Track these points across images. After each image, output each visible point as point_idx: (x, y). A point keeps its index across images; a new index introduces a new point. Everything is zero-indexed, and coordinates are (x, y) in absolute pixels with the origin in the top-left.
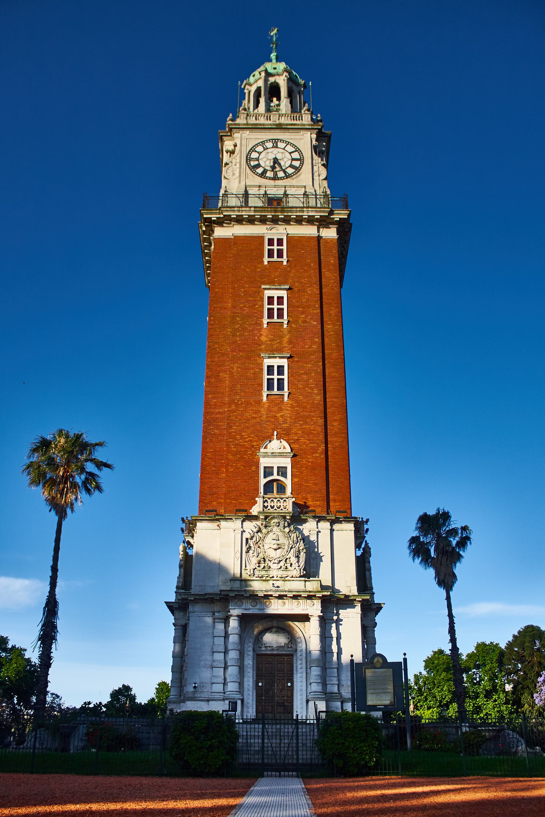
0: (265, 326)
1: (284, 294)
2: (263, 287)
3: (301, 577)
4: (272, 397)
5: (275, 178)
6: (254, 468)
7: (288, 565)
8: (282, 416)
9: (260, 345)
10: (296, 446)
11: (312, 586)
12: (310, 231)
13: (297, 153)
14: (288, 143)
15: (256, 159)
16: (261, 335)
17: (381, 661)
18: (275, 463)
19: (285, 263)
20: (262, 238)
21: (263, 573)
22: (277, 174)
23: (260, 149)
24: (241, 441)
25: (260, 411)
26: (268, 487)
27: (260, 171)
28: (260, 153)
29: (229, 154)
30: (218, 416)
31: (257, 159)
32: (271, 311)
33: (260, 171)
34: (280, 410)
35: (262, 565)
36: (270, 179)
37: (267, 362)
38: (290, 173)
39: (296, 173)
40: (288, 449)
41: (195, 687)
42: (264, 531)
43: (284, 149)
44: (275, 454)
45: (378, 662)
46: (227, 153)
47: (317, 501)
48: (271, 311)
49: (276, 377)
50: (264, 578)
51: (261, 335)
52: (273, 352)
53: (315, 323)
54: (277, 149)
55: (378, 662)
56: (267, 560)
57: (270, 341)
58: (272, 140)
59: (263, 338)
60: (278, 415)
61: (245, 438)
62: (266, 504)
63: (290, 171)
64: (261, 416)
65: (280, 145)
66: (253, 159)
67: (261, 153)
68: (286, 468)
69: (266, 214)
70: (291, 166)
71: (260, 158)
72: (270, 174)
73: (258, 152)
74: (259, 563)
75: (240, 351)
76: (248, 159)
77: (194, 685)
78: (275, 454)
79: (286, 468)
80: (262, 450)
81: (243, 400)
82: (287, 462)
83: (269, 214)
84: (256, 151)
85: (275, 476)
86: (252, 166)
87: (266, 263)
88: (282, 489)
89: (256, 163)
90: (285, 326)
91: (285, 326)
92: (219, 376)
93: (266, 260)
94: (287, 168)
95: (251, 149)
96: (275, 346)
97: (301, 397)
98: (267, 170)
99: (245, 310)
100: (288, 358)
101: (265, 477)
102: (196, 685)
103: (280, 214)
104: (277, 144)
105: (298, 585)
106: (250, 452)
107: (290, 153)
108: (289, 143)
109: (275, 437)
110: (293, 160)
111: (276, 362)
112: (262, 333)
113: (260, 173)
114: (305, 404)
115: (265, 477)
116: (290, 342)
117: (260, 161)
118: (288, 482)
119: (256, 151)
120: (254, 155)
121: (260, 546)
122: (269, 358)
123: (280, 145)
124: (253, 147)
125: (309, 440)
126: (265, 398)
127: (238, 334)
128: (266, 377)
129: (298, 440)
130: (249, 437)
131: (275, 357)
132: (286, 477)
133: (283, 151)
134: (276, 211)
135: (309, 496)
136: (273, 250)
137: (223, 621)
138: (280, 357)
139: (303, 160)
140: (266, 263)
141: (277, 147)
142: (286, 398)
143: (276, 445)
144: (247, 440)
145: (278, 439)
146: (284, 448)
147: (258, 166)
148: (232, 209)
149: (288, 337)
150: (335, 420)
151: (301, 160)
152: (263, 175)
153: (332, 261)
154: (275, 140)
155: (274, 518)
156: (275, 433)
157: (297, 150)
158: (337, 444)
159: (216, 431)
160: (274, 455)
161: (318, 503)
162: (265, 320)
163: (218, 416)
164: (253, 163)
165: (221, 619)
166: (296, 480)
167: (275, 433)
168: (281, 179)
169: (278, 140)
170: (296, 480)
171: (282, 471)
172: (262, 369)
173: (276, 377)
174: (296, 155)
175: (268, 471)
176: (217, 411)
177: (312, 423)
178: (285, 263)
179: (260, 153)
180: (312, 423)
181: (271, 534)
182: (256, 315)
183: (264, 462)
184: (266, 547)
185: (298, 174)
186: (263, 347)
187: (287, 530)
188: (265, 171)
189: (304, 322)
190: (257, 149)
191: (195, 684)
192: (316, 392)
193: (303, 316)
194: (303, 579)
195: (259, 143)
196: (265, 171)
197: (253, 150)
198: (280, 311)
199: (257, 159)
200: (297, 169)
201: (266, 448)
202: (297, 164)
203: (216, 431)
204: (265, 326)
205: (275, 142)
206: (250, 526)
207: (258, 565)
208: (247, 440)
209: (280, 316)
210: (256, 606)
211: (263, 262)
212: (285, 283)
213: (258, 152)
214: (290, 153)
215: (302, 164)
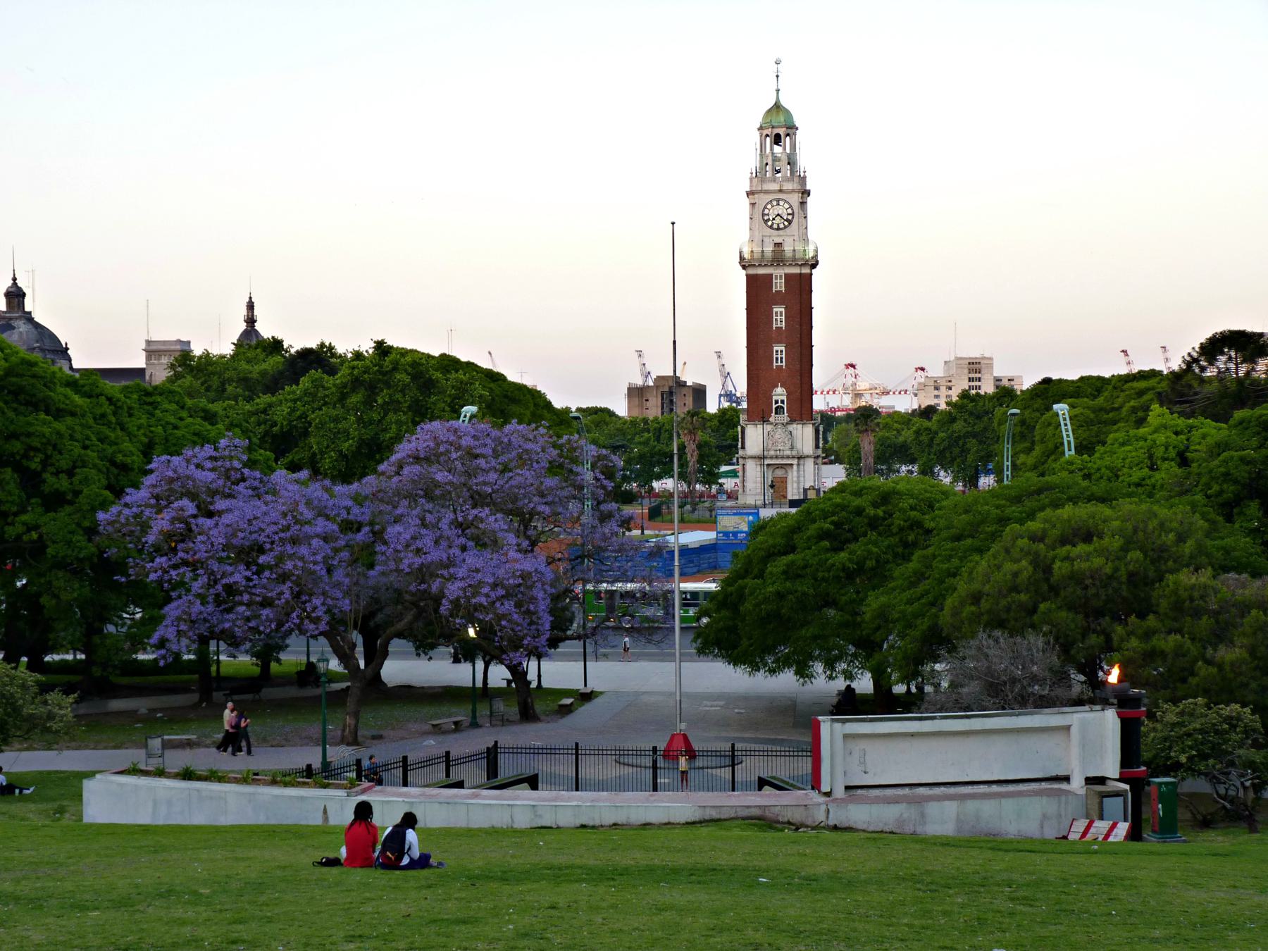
5: (778, 229)
11: (794, 453)
12: (796, 270)
18: (780, 398)
44: (780, 394)
76: (763, 215)
78: (780, 394)
82: (785, 398)
105: (788, 453)
143: (779, 390)
151: (792, 214)
152: (771, 227)
171: (782, 402)
174: (790, 211)
175: (777, 402)
183: (775, 398)
197: (765, 208)
200: (790, 222)
205: (778, 200)
206: (768, 428)
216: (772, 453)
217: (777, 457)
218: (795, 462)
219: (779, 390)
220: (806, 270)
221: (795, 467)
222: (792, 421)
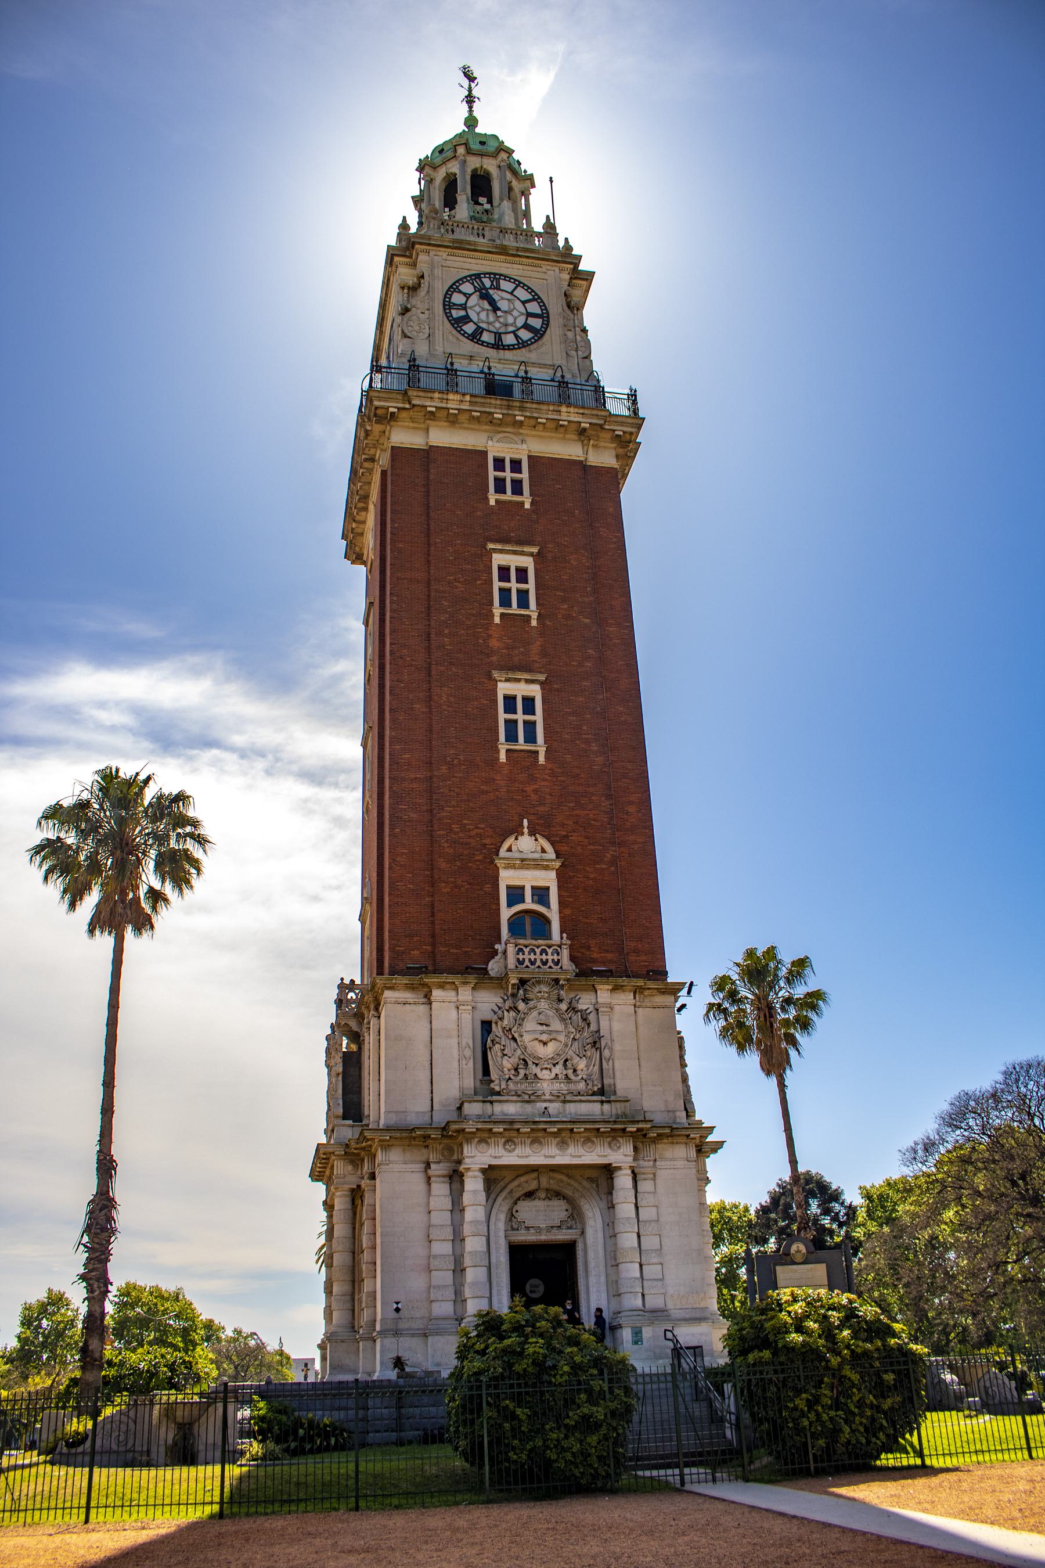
0: (497, 620)
1: (528, 562)
2: (491, 546)
3: (594, 1094)
4: (516, 755)
6: (488, 888)
7: (570, 1072)
8: (536, 791)
9: (488, 656)
10: (564, 848)
12: (571, 450)
13: (535, 303)
14: (519, 284)
15: (461, 305)
16: (490, 636)
17: (804, 1251)
18: (529, 879)
19: (527, 506)
20: (484, 454)
21: (523, 1086)
22: (500, 339)
23: (467, 288)
24: (461, 835)
25: (494, 780)
26: (516, 925)
27: (469, 328)
28: (468, 296)
29: (406, 291)
30: (415, 785)
31: (464, 307)
32: (505, 593)
33: (469, 328)
34: (532, 779)
35: (522, 1072)
36: (488, 345)
37: (504, 688)
38: (525, 339)
39: (536, 341)
40: (551, 854)
41: (397, 1310)
42: (521, 1006)
43: (511, 293)
45: (798, 1251)
46: (403, 288)
47: (608, 951)
48: (505, 593)
49: (520, 717)
50: (526, 1097)
51: (490, 636)
52: (514, 667)
53: (588, 621)
54: (500, 293)
55: (798, 1251)
56: (530, 1063)
57: (507, 648)
58: (490, 274)
59: (494, 643)
60: (528, 789)
61: (470, 830)
62: (521, 957)
63: (525, 335)
64: (497, 790)
65: (505, 285)
66: (455, 305)
67: (470, 295)
68: (548, 888)
69: (492, 410)
70: (526, 326)
71: (469, 304)
72: (486, 337)
73: (465, 294)
74: (516, 1070)
75: (452, 664)
76: (448, 306)
77: (395, 1306)
79: (548, 888)
80: (503, 852)
81: (462, 757)
82: (548, 879)
83: (498, 411)
84: (460, 292)
85: (529, 904)
86: (454, 319)
87: (492, 502)
88: (541, 924)
89: (462, 313)
90: (534, 623)
91: (534, 623)
92: (412, 709)
93: (493, 498)
94: (519, 329)
95: (451, 287)
96: (516, 659)
97: (568, 758)
98: (483, 329)
99: (457, 587)
100: (542, 684)
101: (510, 905)
102: (400, 1306)
103: (517, 413)
104: (498, 284)
106: (480, 857)
107: (524, 303)
108: (520, 282)
109: (526, 830)
110: (529, 315)
111: (521, 689)
112: (490, 632)
113: (470, 332)
114: (577, 771)
115: (510, 905)
116: (544, 653)
117: (469, 311)
118: (553, 914)
119: (460, 292)
120: (457, 299)
121: (516, 1035)
122: (507, 680)
123: (505, 285)
124: (454, 284)
125: (587, 837)
126: (503, 757)
127: (446, 631)
128: (502, 716)
129: (566, 836)
130: (477, 828)
131: (519, 680)
132: (548, 907)
133: (509, 296)
134: (509, 407)
135: (592, 942)
136: (504, 480)
137: (447, 1179)
138: (527, 681)
139: (548, 317)
140: (492, 502)
141: (498, 288)
142: (542, 759)
143: (526, 844)
144: (473, 833)
145: (531, 834)
146: (543, 851)
147: (467, 319)
148: (430, 395)
149: (538, 643)
150: (631, 803)
151: (545, 316)
152: (475, 337)
153: (611, 509)
154: (495, 274)
155: (539, 982)
156: (525, 822)
157: (536, 298)
158: (636, 847)
159: (413, 815)
160: (525, 863)
161: (609, 956)
162: (497, 611)
163: (415, 785)
164: (456, 314)
165: (444, 1176)
166: (568, 912)
167: (525, 822)
168: (509, 348)
169: (501, 275)
170: (568, 912)
171: (541, 894)
172: (496, 701)
173: (520, 717)
174: (534, 308)
175: (516, 894)
176: (413, 776)
177: (591, 806)
178: (527, 506)
179: (468, 296)
180: (591, 806)
181: (535, 1013)
182: (478, 597)
183: (507, 877)
184: (527, 1038)
185: (540, 342)
186: (494, 659)
187: (564, 1006)
188: (479, 331)
189: (568, 617)
190: (462, 288)
191: (397, 1303)
192: (595, 748)
193: (565, 606)
194: (599, 1098)
195: (465, 277)
196: (479, 331)
197: (454, 288)
198: (523, 595)
199: (464, 307)
200: (538, 334)
201: (510, 850)
202: (536, 323)
203: (413, 815)
204: (497, 620)
207: (513, 1072)
208: (473, 833)
209: (523, 603)
210: (514, 1150)
211: (487, 499)
212: (530, 543)
213: (465, 294)
214: (524, 303)
215: (546, 324)
216: (511, 1109)
217: (538, 1131)
218: (621, 1155)
219: (526, 844)
220: (604, 458)
221: (623, 1181)
222: (587, 973)
